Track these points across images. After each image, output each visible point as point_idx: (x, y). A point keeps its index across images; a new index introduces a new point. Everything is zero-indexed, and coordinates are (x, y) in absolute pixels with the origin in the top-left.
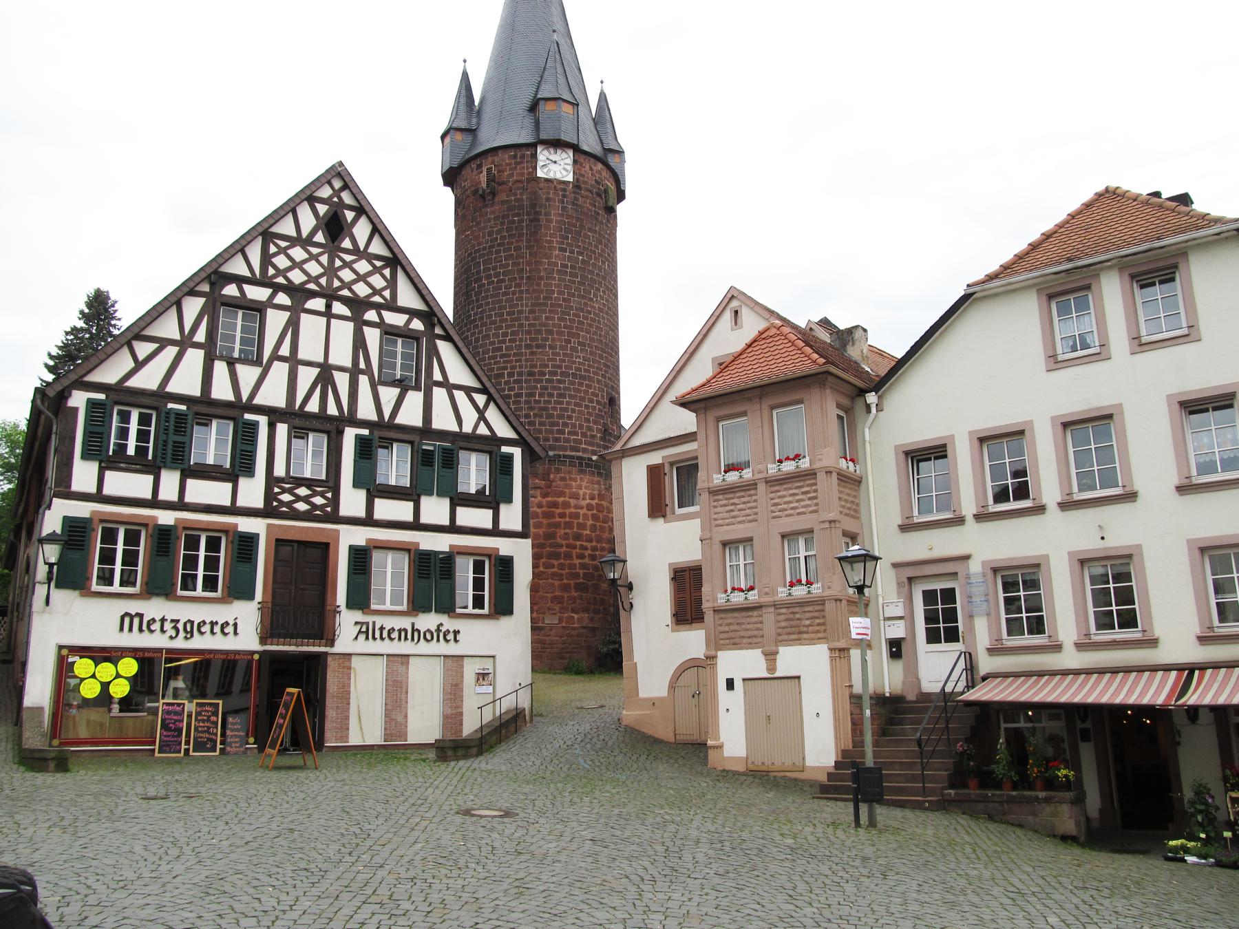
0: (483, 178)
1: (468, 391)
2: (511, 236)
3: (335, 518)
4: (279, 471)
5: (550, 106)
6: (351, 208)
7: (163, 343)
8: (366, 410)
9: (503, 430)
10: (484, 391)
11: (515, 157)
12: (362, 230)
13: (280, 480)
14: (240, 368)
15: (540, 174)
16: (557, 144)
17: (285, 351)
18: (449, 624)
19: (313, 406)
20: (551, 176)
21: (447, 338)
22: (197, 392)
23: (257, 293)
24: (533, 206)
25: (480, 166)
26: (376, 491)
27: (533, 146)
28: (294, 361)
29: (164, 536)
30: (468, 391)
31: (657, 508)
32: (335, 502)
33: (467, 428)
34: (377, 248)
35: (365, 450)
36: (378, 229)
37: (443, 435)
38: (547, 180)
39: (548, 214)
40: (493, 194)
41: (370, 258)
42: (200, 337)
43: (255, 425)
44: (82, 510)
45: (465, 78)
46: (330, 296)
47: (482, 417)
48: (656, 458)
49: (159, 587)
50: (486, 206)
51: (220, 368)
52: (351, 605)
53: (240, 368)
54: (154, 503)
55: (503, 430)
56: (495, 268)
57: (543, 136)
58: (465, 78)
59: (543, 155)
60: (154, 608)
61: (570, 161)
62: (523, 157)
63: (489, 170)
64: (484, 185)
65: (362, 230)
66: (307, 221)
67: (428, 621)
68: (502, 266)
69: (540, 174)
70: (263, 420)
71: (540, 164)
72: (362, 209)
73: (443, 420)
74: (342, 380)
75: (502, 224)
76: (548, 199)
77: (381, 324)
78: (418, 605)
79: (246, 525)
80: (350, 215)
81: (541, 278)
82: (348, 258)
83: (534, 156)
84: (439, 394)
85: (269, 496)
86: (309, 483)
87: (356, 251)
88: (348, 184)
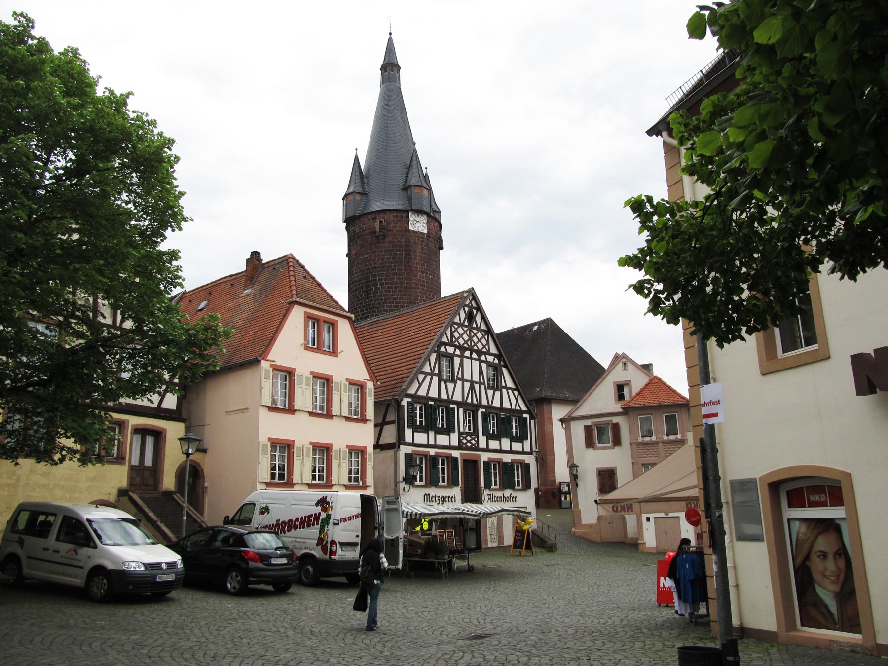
0: (377, 225)
1: (512, 389)
2: (396, 262)
3: (477, 449)
4: (462, 430)
5: (417, 190)
6: (475, 308)
7: (426, 374)
8: (484, 402)
9: (524, 408)
10: (517, 389)
11: (397, 216)
12: (478, 318)
13: (462, 433)
14: (448, 384)
15: (411, 228)
16: (419, 212)
17: (460, 376)
18: (514, 494)
19: (469, 401)
20: (416, 229)
21: (506, 366)
22: (437, 396)
23: (451, 350)
24: (407, 246)
25: (375, 218)
26: (489, 437)
27: (408, 211)
28: (463, 380)
29: (433, 460)
30: (512, 389)
31: (590, 444)
32: (477, 442)
33: (513, 407)
34: (483, 327)
35: (485, 417)
36: (484, 318)
37: (506, 410)
38: (414, 232)
39: (415, 251)
40: (384, 236)
41: (481, 331)
42: (436, 371)
43: (454, 409)
44: (409, 450)
45: (356, 158)
46: (472, 351)
47: (517, 402)
48: (588, 422)
49: (432, 482)
50: (379, 242)
51: (443, 384)
52: (485, 488)
53: (448, 384)
54: (428, 446)
55: (524, 408)
56: (386, 280)
57: (414, 207)
58: (356, 158)
59: (412, 217)
60: (433, 491)
61: (425, 221)
62: (401, 217)
63: (381, 222)
64: (378, 231)
65: (478, 318)
66: (463, 316)
67: (508, 493)
68: (390, 279)
69: (411, 228)
70: (455, 406)
71: (411, 222)
72: (479, 308)
73: (506, 405)
74: (477, 386)
75: (390, 254)
76: (415, 243)
77: (486, 362)
78: (503, 487)
79: (456, 454)
80: (475, 311)
81: (412, 288)
82: (475, 331)
83: (408, 217)
84: (504, 391)
85: (460, 441)
86: (468, 434)
87: (477, 328)
88: (475, 298)
